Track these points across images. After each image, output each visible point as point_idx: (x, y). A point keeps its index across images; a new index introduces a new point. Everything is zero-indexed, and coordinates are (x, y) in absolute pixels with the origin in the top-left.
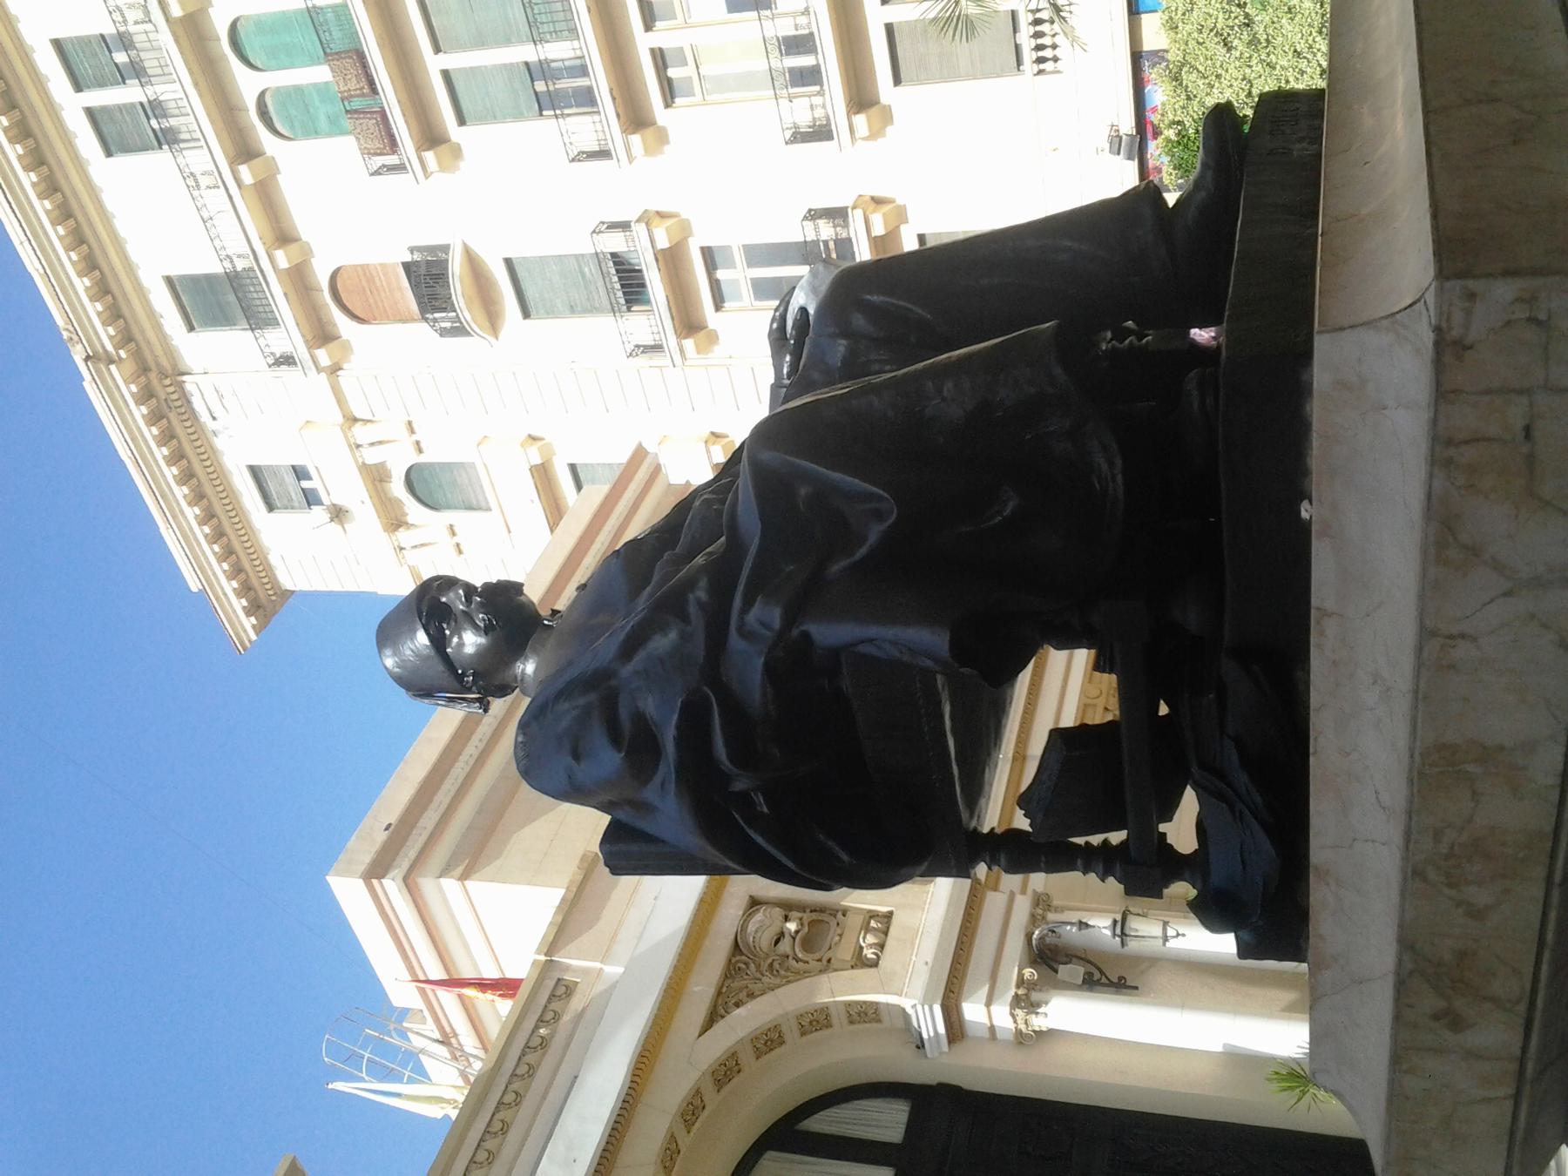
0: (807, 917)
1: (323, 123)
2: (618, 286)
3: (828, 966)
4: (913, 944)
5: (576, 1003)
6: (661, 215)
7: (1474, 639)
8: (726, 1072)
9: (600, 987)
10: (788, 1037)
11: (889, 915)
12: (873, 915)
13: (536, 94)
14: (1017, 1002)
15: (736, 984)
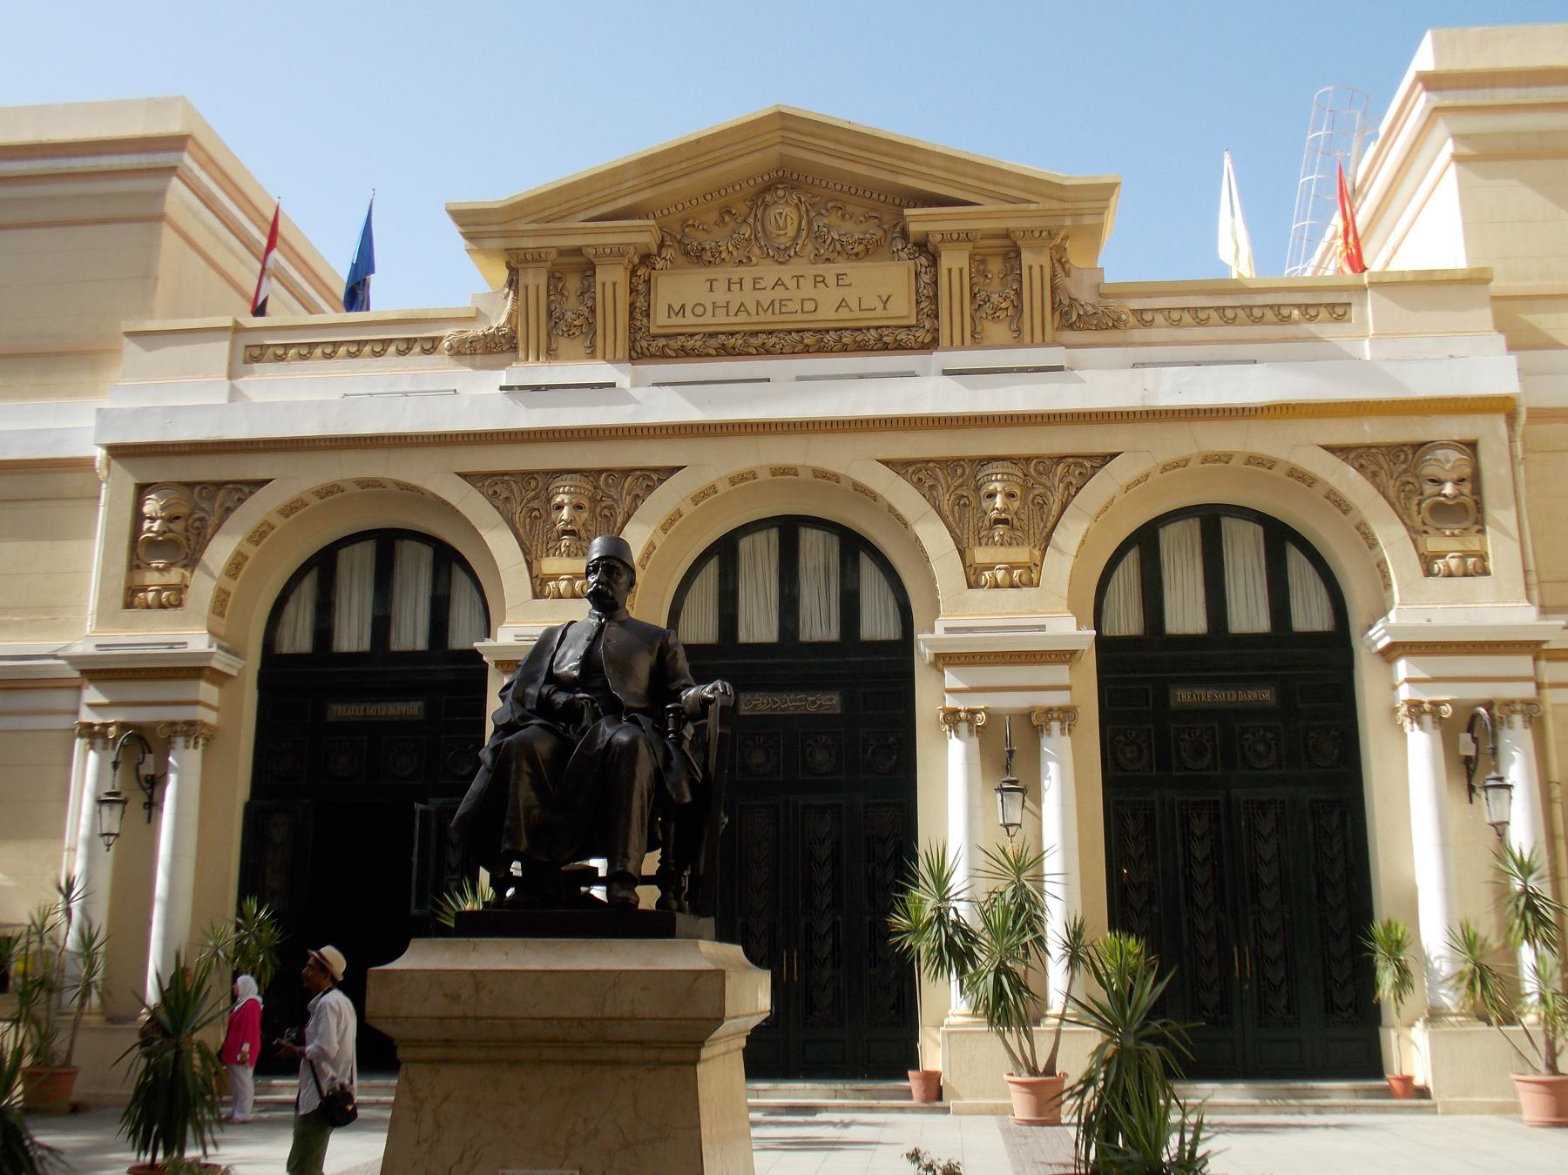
3: (1416, 533)
5: (1328, 330)
9: (1346, 345)
11: (1486, 572)
12: (1483, 557)
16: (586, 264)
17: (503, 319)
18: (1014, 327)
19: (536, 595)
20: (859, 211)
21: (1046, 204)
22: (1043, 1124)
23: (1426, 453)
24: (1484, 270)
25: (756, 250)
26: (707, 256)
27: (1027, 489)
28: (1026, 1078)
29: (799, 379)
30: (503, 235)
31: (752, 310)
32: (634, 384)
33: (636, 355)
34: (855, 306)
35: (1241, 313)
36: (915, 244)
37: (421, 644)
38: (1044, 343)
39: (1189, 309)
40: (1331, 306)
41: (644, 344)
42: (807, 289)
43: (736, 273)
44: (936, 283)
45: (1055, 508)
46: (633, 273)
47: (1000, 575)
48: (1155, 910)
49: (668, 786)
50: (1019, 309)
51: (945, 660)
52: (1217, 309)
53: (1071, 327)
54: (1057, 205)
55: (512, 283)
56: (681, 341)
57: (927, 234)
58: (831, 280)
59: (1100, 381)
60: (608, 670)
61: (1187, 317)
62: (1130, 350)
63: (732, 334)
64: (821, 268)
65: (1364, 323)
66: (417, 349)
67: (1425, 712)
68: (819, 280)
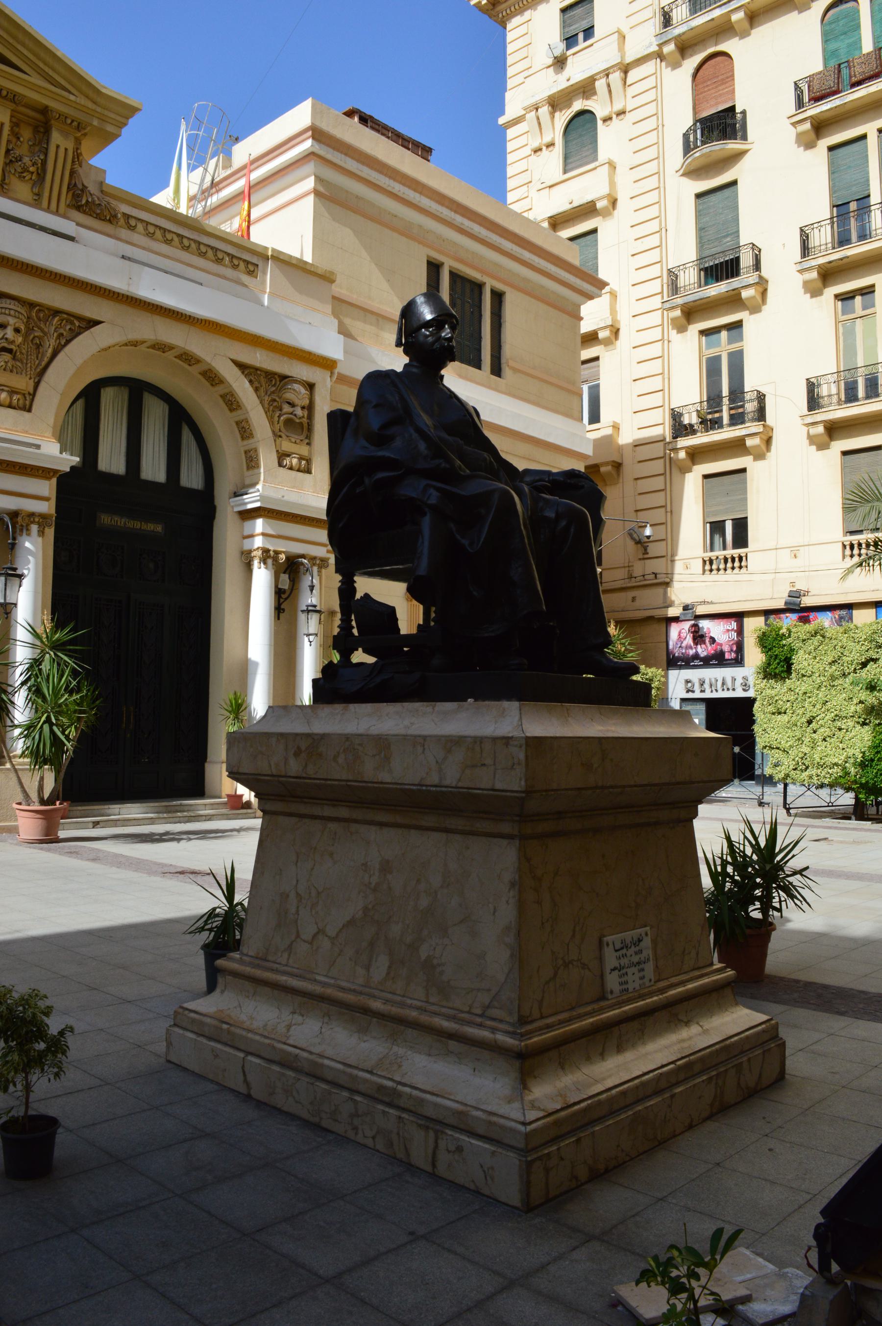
0: (305, 420)
1: (833, 46)
2: (717, 262)
3: (277, 436)
4: (293, 487)
5: (245, 278)
6: (764, 293)
7: (423, 752)
8: (212, 377)
10: (234, 413)
11: (309, 471)
12: (309, 461)
13: (849, 203)
14: (266, 551)
15: (263, 380)
18: (36, 190)
23: (286, 384)
24: (332, 273)
27: (29, 330)
35: (193, 245)
38: (57, 213)
39: (160, 228)
40: (247, 263)
52: (178, 235)
53: (79, 208)
61: (158, 234)
65: (264, 282)
67: (269, 557)
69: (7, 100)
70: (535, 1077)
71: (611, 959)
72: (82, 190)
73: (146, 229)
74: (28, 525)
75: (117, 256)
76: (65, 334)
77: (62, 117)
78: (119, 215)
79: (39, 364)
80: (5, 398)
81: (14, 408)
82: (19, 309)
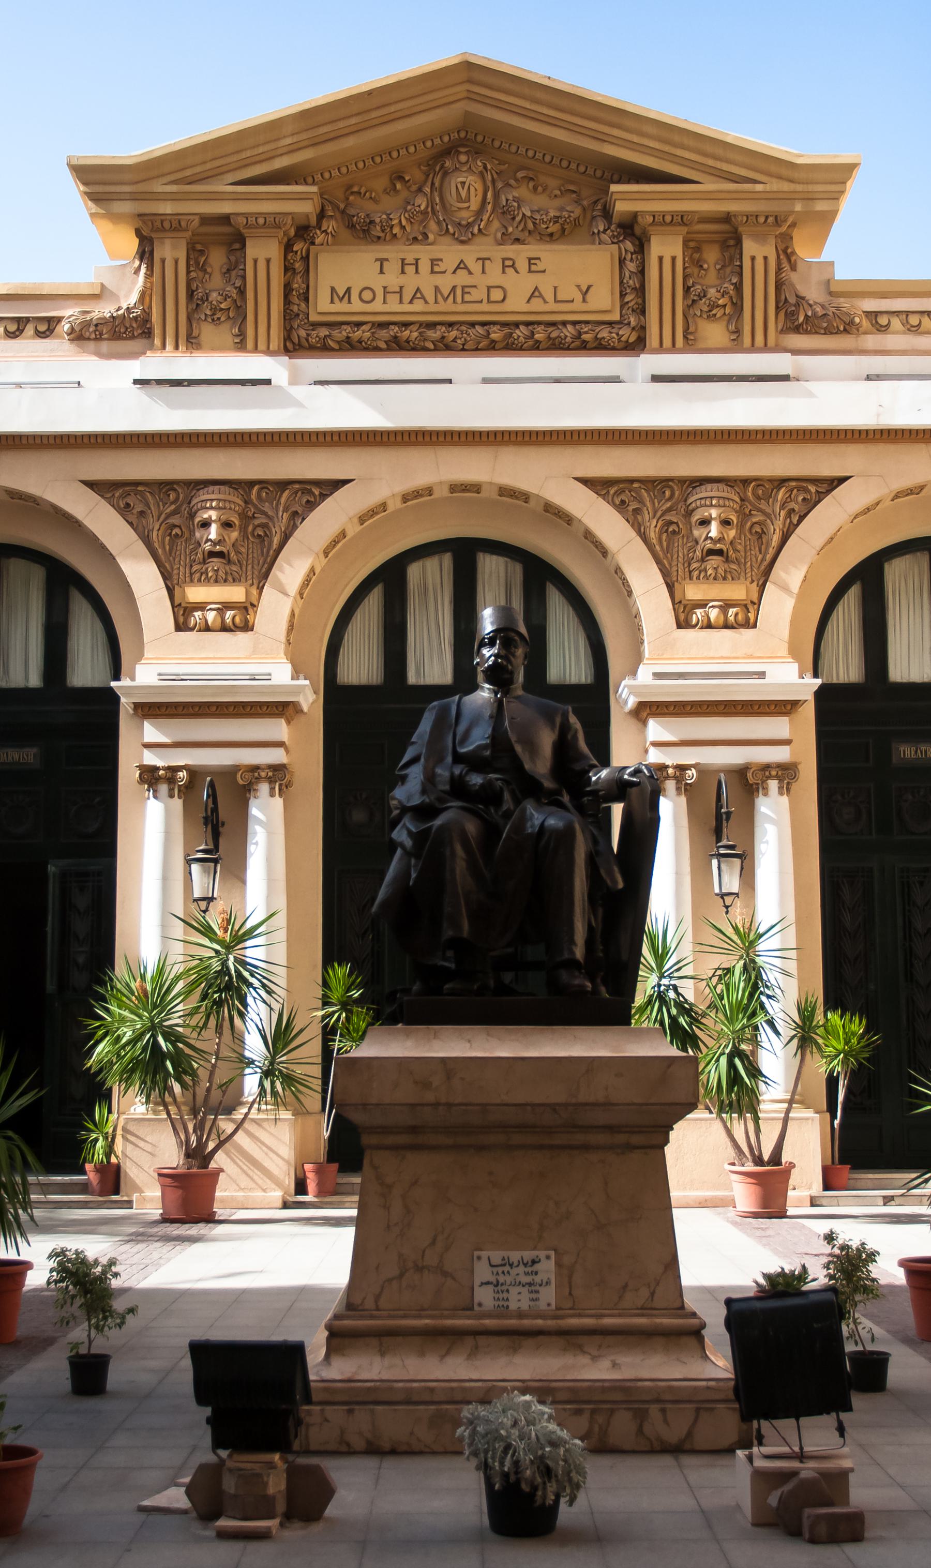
16: (231, 235)
17: (133, 298)
18: (732, 327)
19: (181, 626)
20: (553, 183)
21: (775, 185)
22: (770, 1216)
25: (433, 225)
26: (377, 231)
27: (744, 516)
28: (750, 1167)
29: (486, 381)
30: (135, 197)
31: (430, 297)
32: (294, 380)
33: (293, 347)
34: (549, 296)
36: (620, 225)
37: (35, 680)
38: (766, 348)
41: (303, 333)
42: (494, 275)
43: (411, 252)
44: (642, 272)
45: (776, 539)
46: (288, 248)
47: (714, 614)
48: (872, 987)
49: (602, 872)
50: (738, 306)
51: (647, 710)
53: (798, 329)
54: (786, 186)
55: (146, 253)
56: (346, 331)
57: (635, 215)
58: (522, 265)
59: (829, 393)
60: (518, 748)
62: (863, 358)
63: (406, 325)
64: (510, 250)
66: (30, 330)
68: (508, 265)
69: (674, 225)
70: (344, 1355)
71: (482, 1272)
72: (797, 305)
73: (905, 323)
74: (763, 782)
75: (857, 379)
76: (796, 508)
77: (753, 218)
78: (857, 320)
79: (763, 560)
80: (717, 617)
81: (732, 627)
82: (725, 495)
